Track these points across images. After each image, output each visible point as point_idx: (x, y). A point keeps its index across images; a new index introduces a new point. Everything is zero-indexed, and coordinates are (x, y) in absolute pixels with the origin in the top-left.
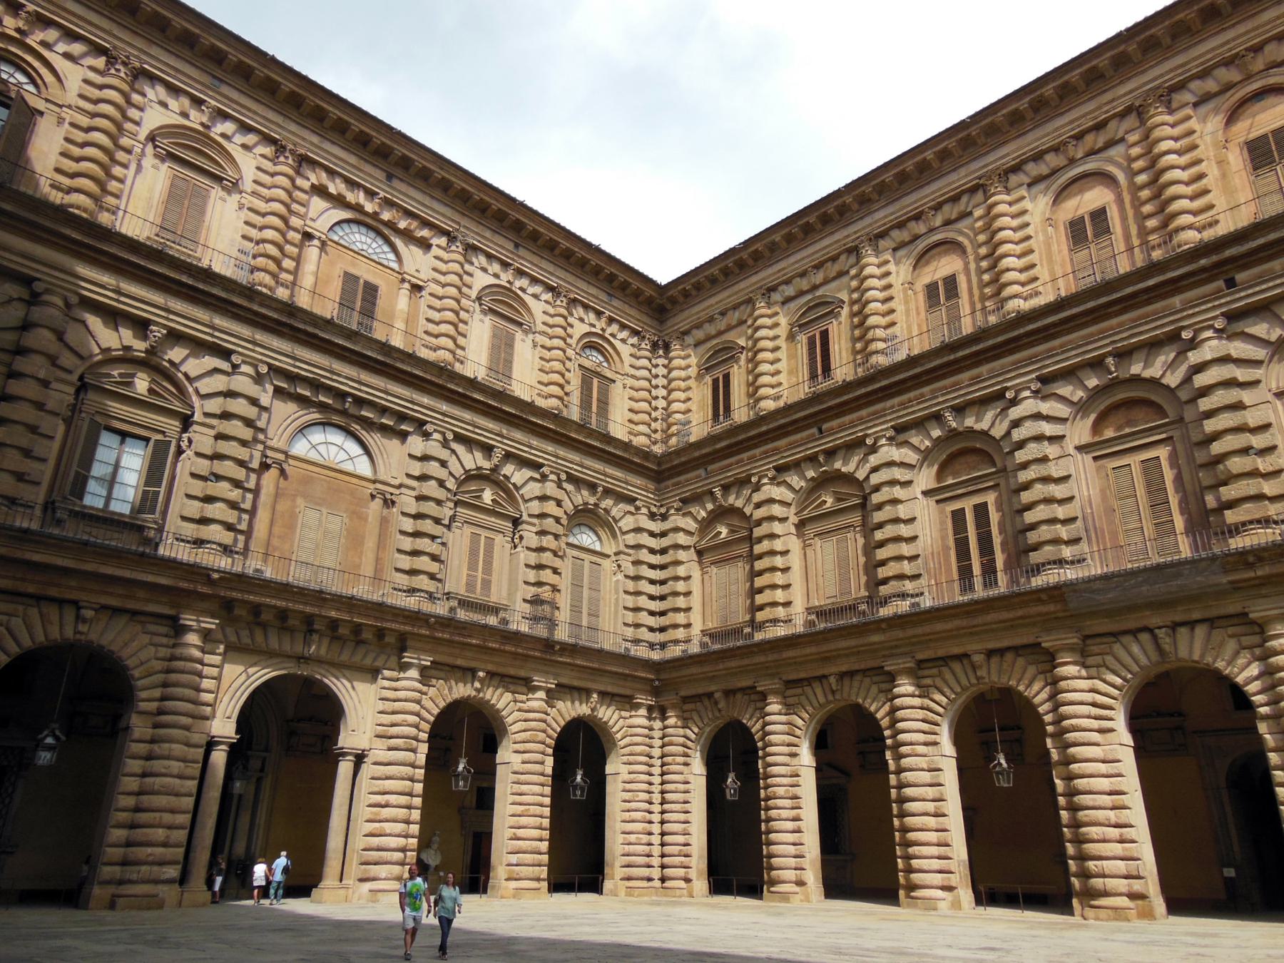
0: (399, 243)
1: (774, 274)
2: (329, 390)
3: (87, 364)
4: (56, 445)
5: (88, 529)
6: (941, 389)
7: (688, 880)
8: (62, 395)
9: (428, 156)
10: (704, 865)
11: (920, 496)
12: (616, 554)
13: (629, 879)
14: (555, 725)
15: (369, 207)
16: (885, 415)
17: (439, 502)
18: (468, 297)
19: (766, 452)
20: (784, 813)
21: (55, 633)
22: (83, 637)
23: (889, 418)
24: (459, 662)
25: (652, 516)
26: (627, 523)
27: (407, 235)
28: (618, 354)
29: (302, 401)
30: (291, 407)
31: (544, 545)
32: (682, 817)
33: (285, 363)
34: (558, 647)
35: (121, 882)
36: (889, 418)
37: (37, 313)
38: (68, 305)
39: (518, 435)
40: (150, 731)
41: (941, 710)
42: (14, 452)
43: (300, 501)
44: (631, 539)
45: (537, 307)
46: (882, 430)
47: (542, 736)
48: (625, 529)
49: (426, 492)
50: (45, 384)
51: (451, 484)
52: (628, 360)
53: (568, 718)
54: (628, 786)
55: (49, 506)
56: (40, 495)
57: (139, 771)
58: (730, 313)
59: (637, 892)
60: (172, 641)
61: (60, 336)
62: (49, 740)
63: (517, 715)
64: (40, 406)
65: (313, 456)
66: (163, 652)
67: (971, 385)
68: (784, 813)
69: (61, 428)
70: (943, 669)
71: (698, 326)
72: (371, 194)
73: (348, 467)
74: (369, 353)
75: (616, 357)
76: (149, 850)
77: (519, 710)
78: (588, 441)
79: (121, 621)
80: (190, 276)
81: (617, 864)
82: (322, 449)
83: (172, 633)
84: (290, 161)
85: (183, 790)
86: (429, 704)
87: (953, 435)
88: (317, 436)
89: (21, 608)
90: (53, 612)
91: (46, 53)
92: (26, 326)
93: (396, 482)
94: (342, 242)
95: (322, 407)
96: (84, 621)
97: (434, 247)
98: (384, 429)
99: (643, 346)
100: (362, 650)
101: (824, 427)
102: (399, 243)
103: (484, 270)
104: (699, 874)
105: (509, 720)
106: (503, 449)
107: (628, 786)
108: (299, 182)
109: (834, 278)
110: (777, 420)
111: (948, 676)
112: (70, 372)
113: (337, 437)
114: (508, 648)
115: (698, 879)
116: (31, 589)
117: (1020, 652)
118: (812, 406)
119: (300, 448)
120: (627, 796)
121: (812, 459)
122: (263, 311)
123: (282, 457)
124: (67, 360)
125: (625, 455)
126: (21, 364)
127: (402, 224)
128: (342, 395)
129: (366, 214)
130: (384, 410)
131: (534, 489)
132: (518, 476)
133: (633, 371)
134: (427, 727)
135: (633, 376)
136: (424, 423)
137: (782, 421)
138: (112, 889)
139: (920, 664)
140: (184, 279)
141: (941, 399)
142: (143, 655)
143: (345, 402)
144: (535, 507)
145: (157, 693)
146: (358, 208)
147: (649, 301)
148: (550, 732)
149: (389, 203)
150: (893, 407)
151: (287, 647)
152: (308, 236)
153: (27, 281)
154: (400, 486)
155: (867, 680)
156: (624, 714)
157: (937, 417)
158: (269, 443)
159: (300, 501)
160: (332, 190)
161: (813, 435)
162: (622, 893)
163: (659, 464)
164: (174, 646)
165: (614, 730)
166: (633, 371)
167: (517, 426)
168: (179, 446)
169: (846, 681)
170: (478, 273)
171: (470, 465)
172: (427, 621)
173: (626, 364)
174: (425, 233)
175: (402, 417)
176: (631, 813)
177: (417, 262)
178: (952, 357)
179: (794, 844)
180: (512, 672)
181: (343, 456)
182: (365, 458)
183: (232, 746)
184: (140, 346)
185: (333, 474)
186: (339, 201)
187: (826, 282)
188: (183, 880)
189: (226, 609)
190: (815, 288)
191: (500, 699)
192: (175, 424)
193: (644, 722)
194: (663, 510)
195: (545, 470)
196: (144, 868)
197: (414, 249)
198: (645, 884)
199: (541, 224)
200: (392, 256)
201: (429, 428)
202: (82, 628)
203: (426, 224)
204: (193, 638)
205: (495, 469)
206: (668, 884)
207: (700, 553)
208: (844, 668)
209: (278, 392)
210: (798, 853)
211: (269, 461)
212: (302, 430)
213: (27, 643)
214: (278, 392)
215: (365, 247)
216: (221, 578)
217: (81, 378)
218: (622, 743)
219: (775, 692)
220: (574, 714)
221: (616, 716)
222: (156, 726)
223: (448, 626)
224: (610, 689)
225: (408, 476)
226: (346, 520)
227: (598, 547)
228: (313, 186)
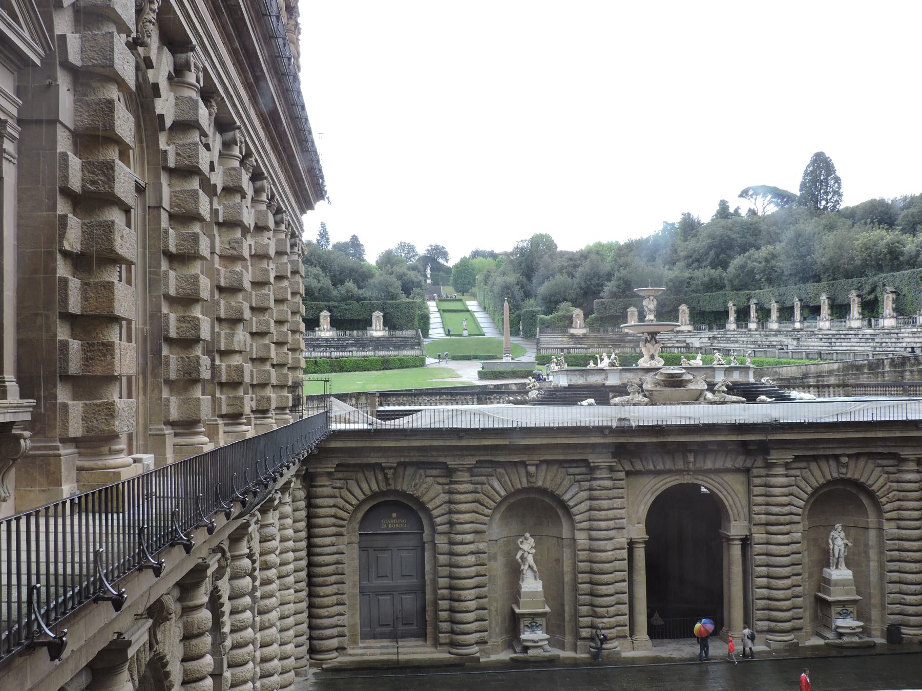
22: (533, 485)
60: (589, 477)
183: (645, 542)
188: (632, 632)
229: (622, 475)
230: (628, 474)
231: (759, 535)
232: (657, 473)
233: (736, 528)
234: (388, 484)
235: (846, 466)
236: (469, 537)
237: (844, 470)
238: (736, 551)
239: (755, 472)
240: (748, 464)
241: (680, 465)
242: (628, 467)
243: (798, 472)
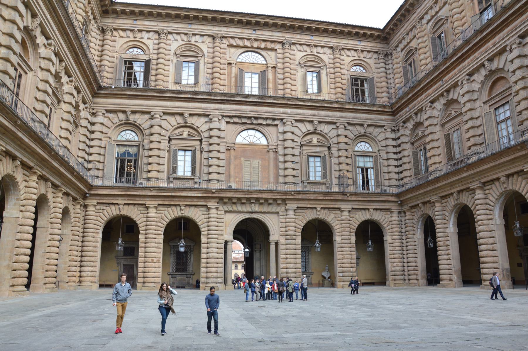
1: (420, 11)
2: (245, 117)
3: (170, 131)
4: (166, 159)
5: (181, 182)
6: (481, 52)
7: (417, 280)
8: (164, 145)
9: (265, 17)
10: (425, 274)
11: (482, 105)
12: (379, 151)
13: (395, 280)
14: (354, 224)
16: (463, 70)
17: (293, 148)
18: (294, 64)
19: (426, 96)
20: (443, 252)
21: (176, 215)
22: (183, 215)
23: (465, 70)
24: (309, 206)
25: (393, 131)
27: (265, 49)
28: (369, 65)
31: (340, 155)
32: (414, 255)
33: (227, 113)
34: (348, 195)
35: (207, 283)
36: (465, 70)
37: (154, 122)
38: (161, 116)
39: (323, 113)
40: (207, 240)
41: (492, 204)
42: (155, 164)
43: (242, 159)
44: (384, 143)
46: (463, 77)
47: (348, 229)
48: (381, 140)
49: (286, 145)
50: (159, 142)
51: (296, 139)
52: (373, 66)
53: (361, 221)
54: (392, 245)
55: (168, 178)
56: (164, 176)
57: (206, 252)
58: (410, 33)
59: (397, 285)
60: (208, 213)
61: (160, 126)
62: (182, 244)
63: (337, 222)
64: (159, 149)
65: (245, 142)
66: (206, 216)
67: (492, 47)
68: (443, 252)
69: (167, 154)
70: (492, 185)
71: (400, 42)
73: (258, 142)
74: (255, 100)
75: (368, 67)
76: (212, 274)
77: (338, 220)
78: (355, 108)
79: (192, 208)
80: (191, 95)
81: (390, 275)
82: (248, 138)
83: (207, 210)
85: (219, 257)
86: (300, 223)
87: (492, 72)
88: (244, 134)
89: (166, 208)
90: (174, 208)
91: (143, 40)
92: (152, 127)
93: (276, 144)
94: (243, 61)
96: (182, 210)
97: (277, 50)
99: (380, 58)
100: (270, 207)
101: (444, 79)
104: (423, 277)
105: (334, 225)
106: (317, 121)
107: (392, 245)
108: (223, 46)
109: (443, 6)
110: (426, 81)
111: (494, 188)
112: (165, 136)
114: (327, 198)
115: (422, 279)
116: (167, 203)
117: (520, 174)
118: (436, 72)
119: (239, 140)
120: (392, 249)
121: (442, 95)
122: (216, 98)
123: (233, 145)
124: (163, 132)
125: (375, 109)
126: (152, 138)
128: (249, 118)
129: (249, 47)
130: (267, 119)
131: (334, 133)
132: (325, 129)
133: (376, 70)
134: (300, 231)
135: (377, 73)
136: (282, 120)
137: (428, 81)
138: (205, 285)
139: (484, 184)
140: (189, 96)
141: (482, 57)
142: (200, 218)
143: (251, 120)
144: (335, 140)
145: (206, 229)
147: (379, 37)
148: (353, 227)
150: (465, 65)
151: (244, 209)
153: (149, 113)
154: (277, 145)
155: (467, 193)
156: (387, 216)
157: (483, 65)
158: (228, 142)
159: (242, 159)
161: (440, 84)
162: (392, 285)
163: (392, 109)
164: (209, 214)
165: (383, 223)
166: (376, 70)
167: (322, 110)
168: (201, 150)
169: (461, 194)
170: (299, 53)
171: (304, 130)
172: (291, 193)
173: (373, 68)
175: (274, 119)
176: (394, 255)
178: (482, 36)
179: (448, 265)
180: (332, 206)
181: (255, 139)
182: (264, 137)
185: (253, 147)
186: (238, 46)
187: (440, 9)
189: (221, 200)
190: (437, 13)
191: (330, 217)
192: (198, 143)
193: (397, 218)
194: (397, 128)
195: (338, 124)
196: (211, 279)
197: (270, 53)
198: (402, 282)
199: (318, 24)
200: (263, 59)
201: (284, 121)
202: (182, 212)
204: (213, 211)
206: (411, 281)
207: (412, 144)
208: (458, 189)
209: (228, 123)
210: (449, 268)
211: (229, 148)
213: (170, 218)
214: (228, 123)
215: (252, 59)
216: (216, 191)
217: (169, 137)
218: (387, 228)
219: (437, 201)
220: (363, 219)
221: (383, 218)
222: (208, 239)
223: (300, 194)
224: (378, 207)
226: (260, 162)
227: (370, 150)
228: (228, 46)
229: (223, 212)
230: (226, 212)
231: (282, 241)
232: (240, 212)
233: (273, 237)
234: (120, 211)
235: (319, 211)
236: (154, 236)
237: (318, 213)
238: (273, 247)
239: (281, 214)
240: (277, 211)
241: (249, 209)
242: (226, 209)
243: (300, 214)
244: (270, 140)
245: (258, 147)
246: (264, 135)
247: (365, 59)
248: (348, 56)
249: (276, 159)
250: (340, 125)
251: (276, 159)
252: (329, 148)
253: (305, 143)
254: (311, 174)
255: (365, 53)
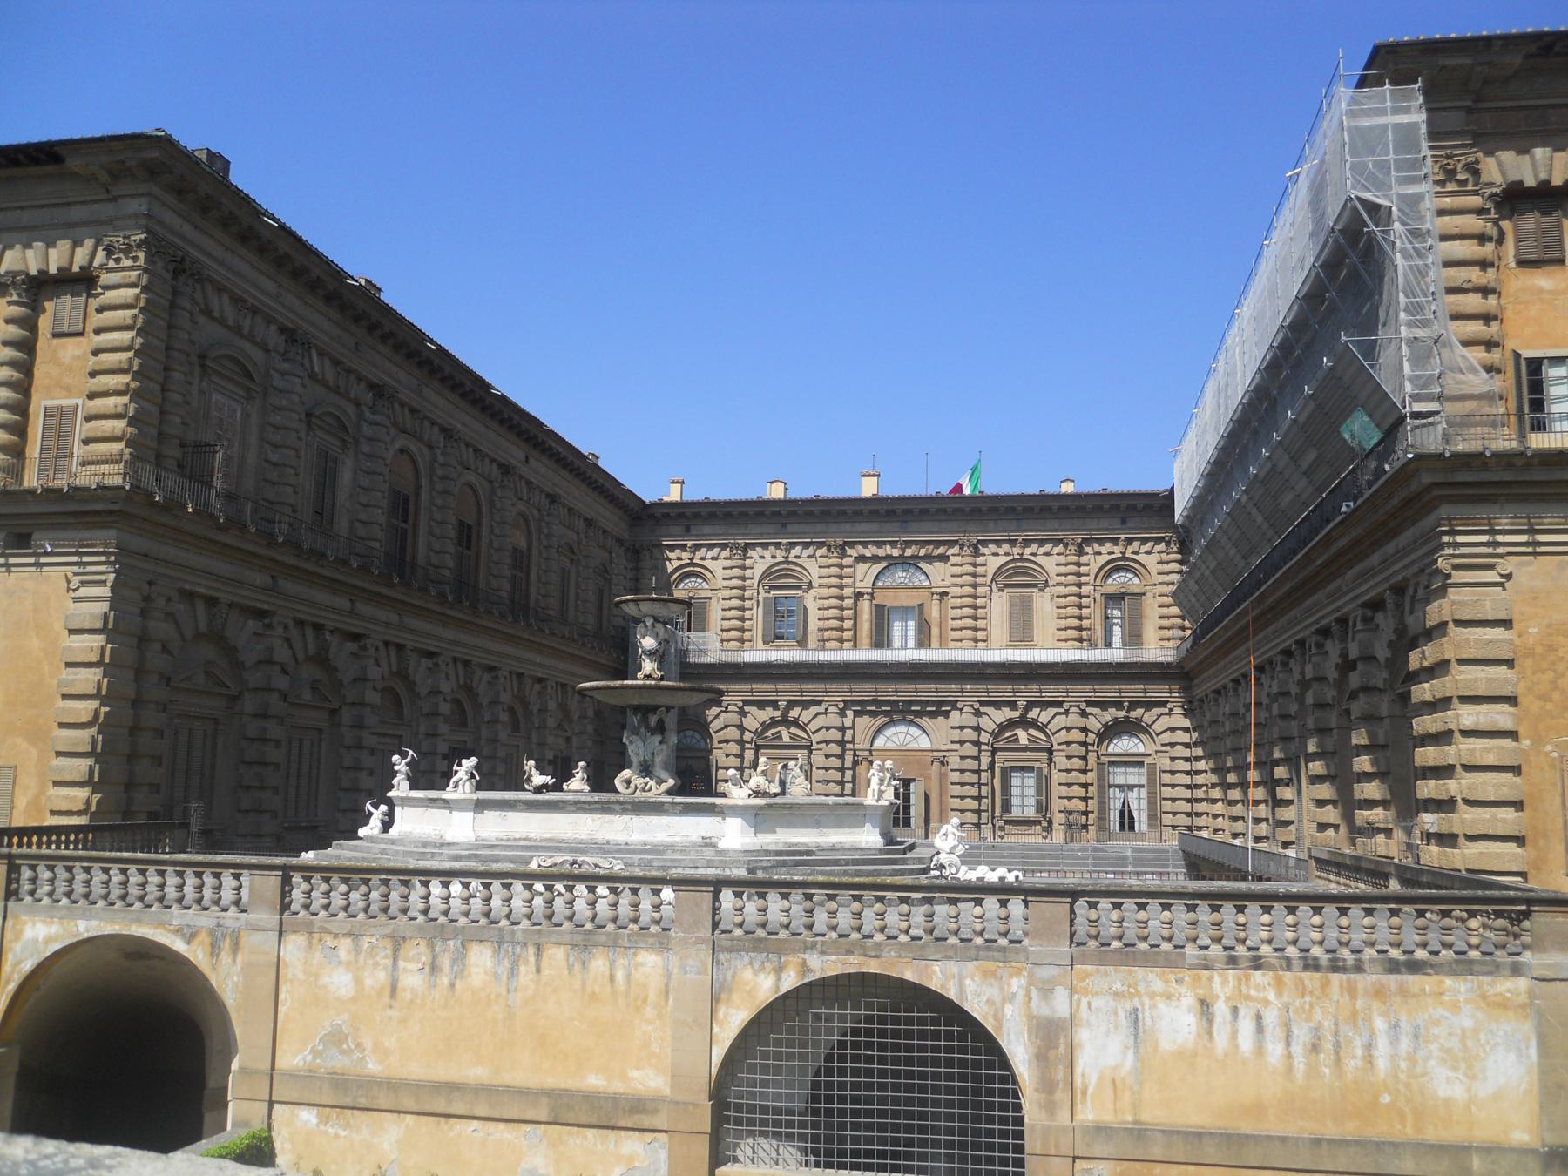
0: (922, 565)
15: (896, 552)
26: (1165, 722)
27: (929, 558)
29: (873, 714)
30: (866, 718)
33: (856, 696)
44: (1167, 737)
45: (1050, 564)
65: (890, 745)
72: (893, 544)
73: (914, 745)
84: (835, 554)
88: (890, 731)
95: (886, 713)
98: (933, 715)
102: (922, 565)
103: (996, 554)
113: (902, 728)
127: (922, 552)
131: (1061, 721)
146: (888, 557)
149: (908, 544)
152: (858, 595)
160: (868, 554)
173: (1154, 573)
174: (941, 550)
177: (939, 574)
182: (924, 735)
184: (777, 714)
186: (875, 559)
201: (959, 705)
203: (938, 544)
205: (1023, 717)
212: (879, 731)
214: (857, 714)
215: (902, 580)
225: (952, 742)
244: (934, 740)
245: (913, 753)
246: (925, 731)
247: (1135, 557)
248: (1100, 554)
249: (943, 777)
250: (1071, 706)
251: (943, 777)
252: (1050, 751)
253: (1001, 744)
254: (1015, 801)
255: (1136, 544)
